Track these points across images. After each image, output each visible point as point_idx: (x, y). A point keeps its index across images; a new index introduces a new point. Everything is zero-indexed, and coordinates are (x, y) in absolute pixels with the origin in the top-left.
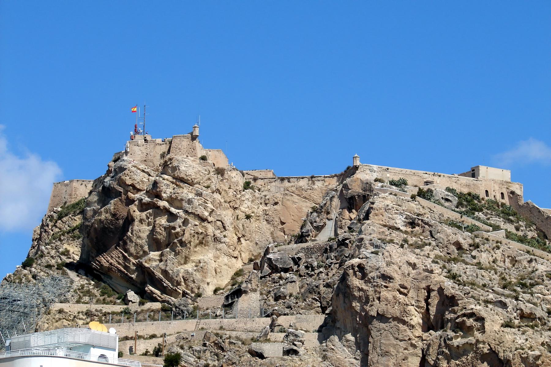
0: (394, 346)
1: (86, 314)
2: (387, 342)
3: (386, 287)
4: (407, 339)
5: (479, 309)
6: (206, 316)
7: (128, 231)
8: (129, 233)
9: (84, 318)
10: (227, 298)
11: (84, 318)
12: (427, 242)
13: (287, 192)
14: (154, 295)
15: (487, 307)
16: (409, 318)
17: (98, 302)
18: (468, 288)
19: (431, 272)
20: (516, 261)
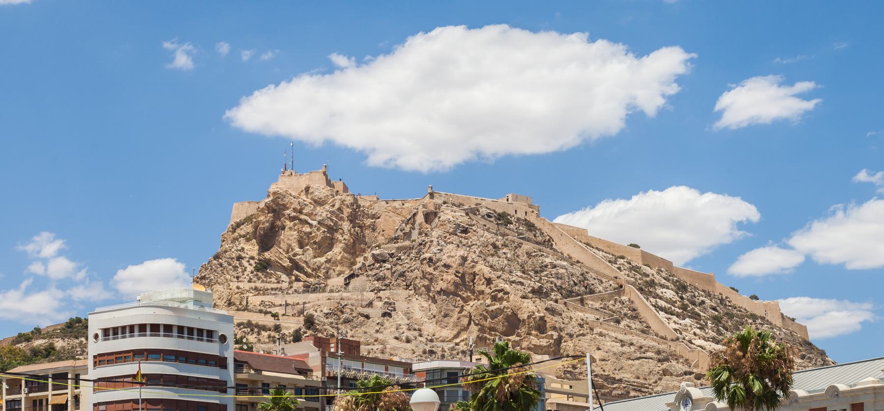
0: (452, 311)
1: (255, 289)
2: (448, 308)
3: (447, 272)
4: (460, 306)
5: (507, 287)
6: (332, 291)
7: (281, 235)
8: (282, 237)
9: (253, 292)
10: (345, 279)
11: (253, 292)
12: (474, 243)
13: (386, 210)
14: (299, 277)
15: (511, 285)
16: (462, 293)
17: (263, 281)
18: (500, 273)
19: (477, 262)
20: (532, 256)
